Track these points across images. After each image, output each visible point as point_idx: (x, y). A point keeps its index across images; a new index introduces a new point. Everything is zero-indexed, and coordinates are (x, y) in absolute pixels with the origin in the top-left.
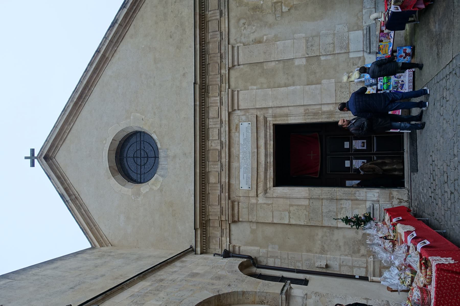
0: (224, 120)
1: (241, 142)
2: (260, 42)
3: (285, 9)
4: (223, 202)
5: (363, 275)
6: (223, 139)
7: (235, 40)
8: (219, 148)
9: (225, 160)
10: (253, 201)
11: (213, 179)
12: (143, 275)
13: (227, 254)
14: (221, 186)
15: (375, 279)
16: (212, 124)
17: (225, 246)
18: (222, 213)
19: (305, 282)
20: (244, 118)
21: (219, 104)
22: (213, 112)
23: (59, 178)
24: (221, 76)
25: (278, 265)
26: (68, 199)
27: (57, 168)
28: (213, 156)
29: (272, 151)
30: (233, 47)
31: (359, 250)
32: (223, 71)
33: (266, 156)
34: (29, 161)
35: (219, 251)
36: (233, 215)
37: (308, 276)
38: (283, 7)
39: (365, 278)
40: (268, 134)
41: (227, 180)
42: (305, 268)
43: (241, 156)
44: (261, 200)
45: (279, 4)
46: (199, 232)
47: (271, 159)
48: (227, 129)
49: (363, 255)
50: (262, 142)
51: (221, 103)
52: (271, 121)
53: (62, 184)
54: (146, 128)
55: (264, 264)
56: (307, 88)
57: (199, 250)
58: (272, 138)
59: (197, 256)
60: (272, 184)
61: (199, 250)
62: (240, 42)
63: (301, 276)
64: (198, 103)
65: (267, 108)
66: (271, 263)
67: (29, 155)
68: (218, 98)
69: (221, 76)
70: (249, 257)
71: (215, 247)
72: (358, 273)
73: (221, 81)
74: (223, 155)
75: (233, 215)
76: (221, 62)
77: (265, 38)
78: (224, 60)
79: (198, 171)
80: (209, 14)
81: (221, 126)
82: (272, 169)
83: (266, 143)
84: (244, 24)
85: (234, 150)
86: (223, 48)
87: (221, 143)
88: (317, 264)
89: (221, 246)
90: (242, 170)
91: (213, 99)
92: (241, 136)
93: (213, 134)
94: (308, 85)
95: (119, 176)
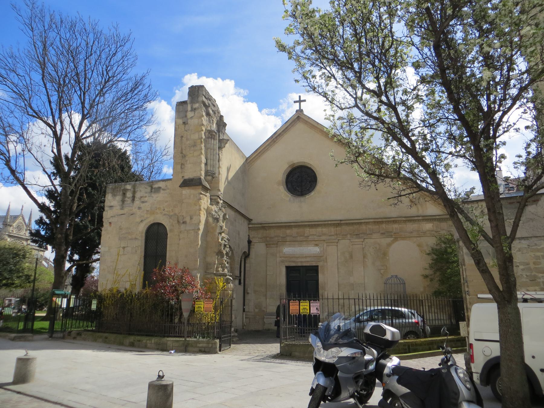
0: (321, 237)
1: (309, 248)
2: (364, 257)
3: (382, 271)
4: (276, 238)
5: (246, 310)
6: (310, 237)
7: (367, 242)
8: (306, 235)
9: (299, 239)
10: (278, 255)
11: (288, 231)
12: (237, 211)
13: (249, 242)
14: (284, 237)
15: (244, 315)
16: (319, 230)
17: (253, 240)
18: (271, 238)
19: (240, 283)
20: (322, 249)
21: (329, 234)
22: (325, 230)
23: (286, 128)
24: (346, 235)
25: (247, 269)
26: (274, 138)
27: (293, 125)
28: (301, 230)
29: (304, 265)
30: (363, 242)
31: (257, 308)
32: (349, 236)
33: (301, 262)
34: (298, 100)
35: (251, 236)
36: (270, 244)
37: (242, 284)
38: (383, 270)
39: (244, 310)
40: (313, 263)
41: (288, 240)
42: (246, 282)
43: (301, 248)
44: (278, 259)
45: (386, 268)
46: (260, 226)
47: (299, 264)
48: (316, 239)
49: (254, 310)
50: (308, 259)
51: (330, 236)
52: (320, 264)
53: (283, 131)
54: (319, 186)
55: (247, 261)
56: (337, 284)
57: (251, 226)
58: (311, 265)
59: (247, 224)
60: (287, 265)
61: (251, 226)
62: (365, 246)
63: (242, 281)
64: (329, 222)
65: (327, 262)
66: (247, 265)
67: (302, 99)
68: (333, 234)
69: (346, 235)
70: (249, 254)
71: (253, 234)
72: (246, 307)
73: (343, 235)
74: (301, 238)
75: (270, 244)
76: (354, 235)
77: (367, 260)
78: (355, 236)
79: (292, 224)
80: (384, 226)
81: (317, 236)
82: (295, 265)
83: (308, 262)
84: (376, 248)
85: (305, 243)
86: (362, 235)
87: (308, 236)
88: (248, 289)
89: (254, 237)
90: (293, 249)
91: (333, 230)
92: (312, 248)
93: (313, 231)
94: (338, 284)
95: (290, 169)
